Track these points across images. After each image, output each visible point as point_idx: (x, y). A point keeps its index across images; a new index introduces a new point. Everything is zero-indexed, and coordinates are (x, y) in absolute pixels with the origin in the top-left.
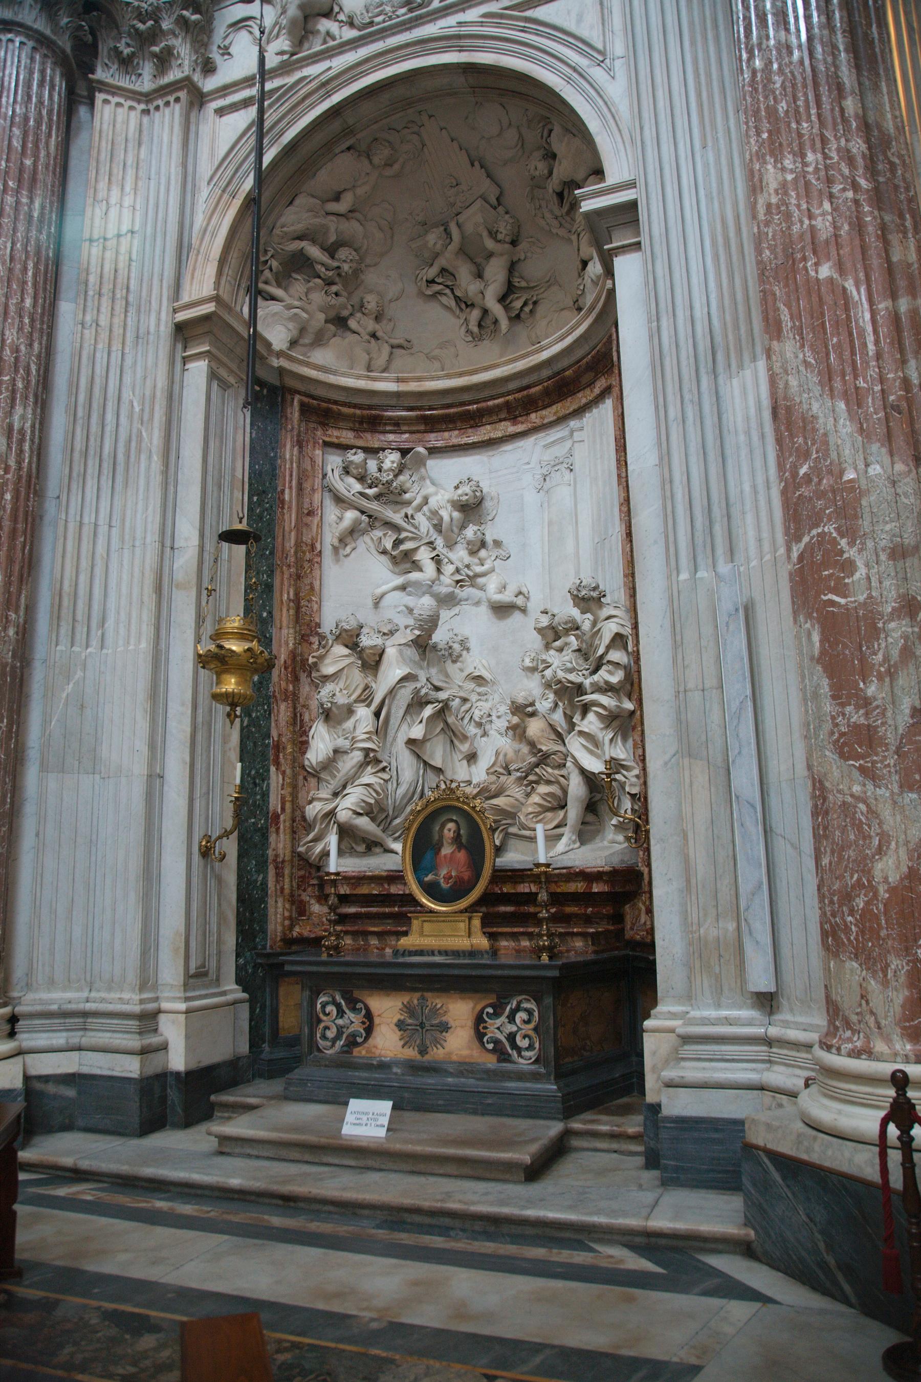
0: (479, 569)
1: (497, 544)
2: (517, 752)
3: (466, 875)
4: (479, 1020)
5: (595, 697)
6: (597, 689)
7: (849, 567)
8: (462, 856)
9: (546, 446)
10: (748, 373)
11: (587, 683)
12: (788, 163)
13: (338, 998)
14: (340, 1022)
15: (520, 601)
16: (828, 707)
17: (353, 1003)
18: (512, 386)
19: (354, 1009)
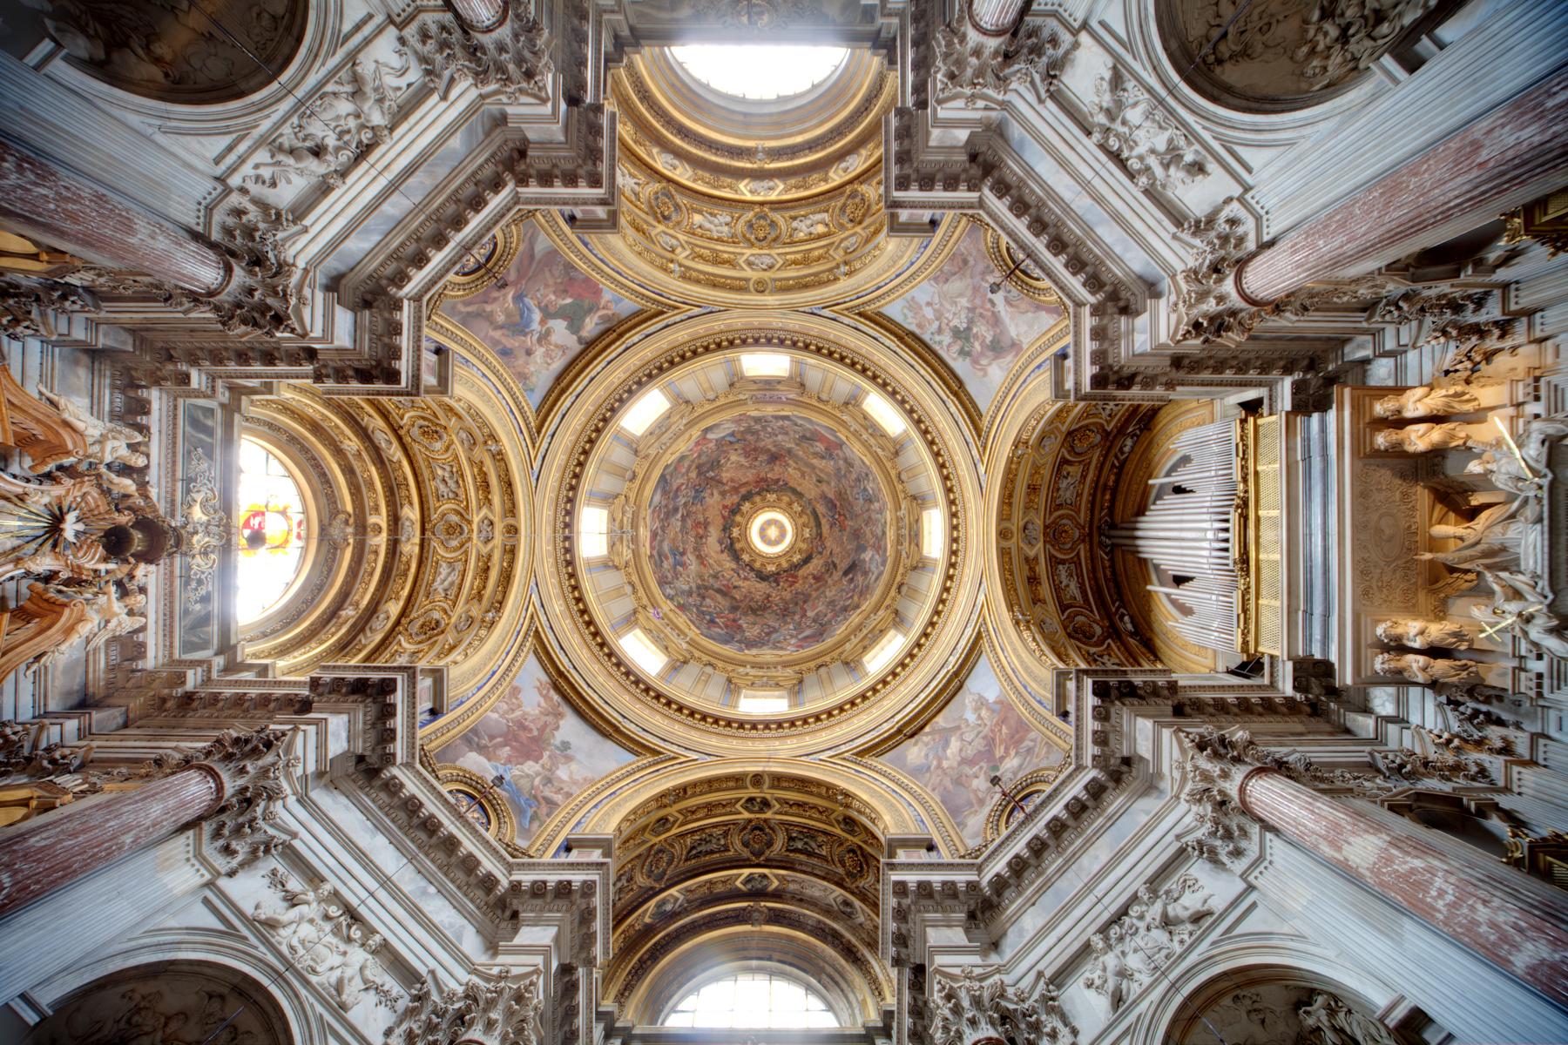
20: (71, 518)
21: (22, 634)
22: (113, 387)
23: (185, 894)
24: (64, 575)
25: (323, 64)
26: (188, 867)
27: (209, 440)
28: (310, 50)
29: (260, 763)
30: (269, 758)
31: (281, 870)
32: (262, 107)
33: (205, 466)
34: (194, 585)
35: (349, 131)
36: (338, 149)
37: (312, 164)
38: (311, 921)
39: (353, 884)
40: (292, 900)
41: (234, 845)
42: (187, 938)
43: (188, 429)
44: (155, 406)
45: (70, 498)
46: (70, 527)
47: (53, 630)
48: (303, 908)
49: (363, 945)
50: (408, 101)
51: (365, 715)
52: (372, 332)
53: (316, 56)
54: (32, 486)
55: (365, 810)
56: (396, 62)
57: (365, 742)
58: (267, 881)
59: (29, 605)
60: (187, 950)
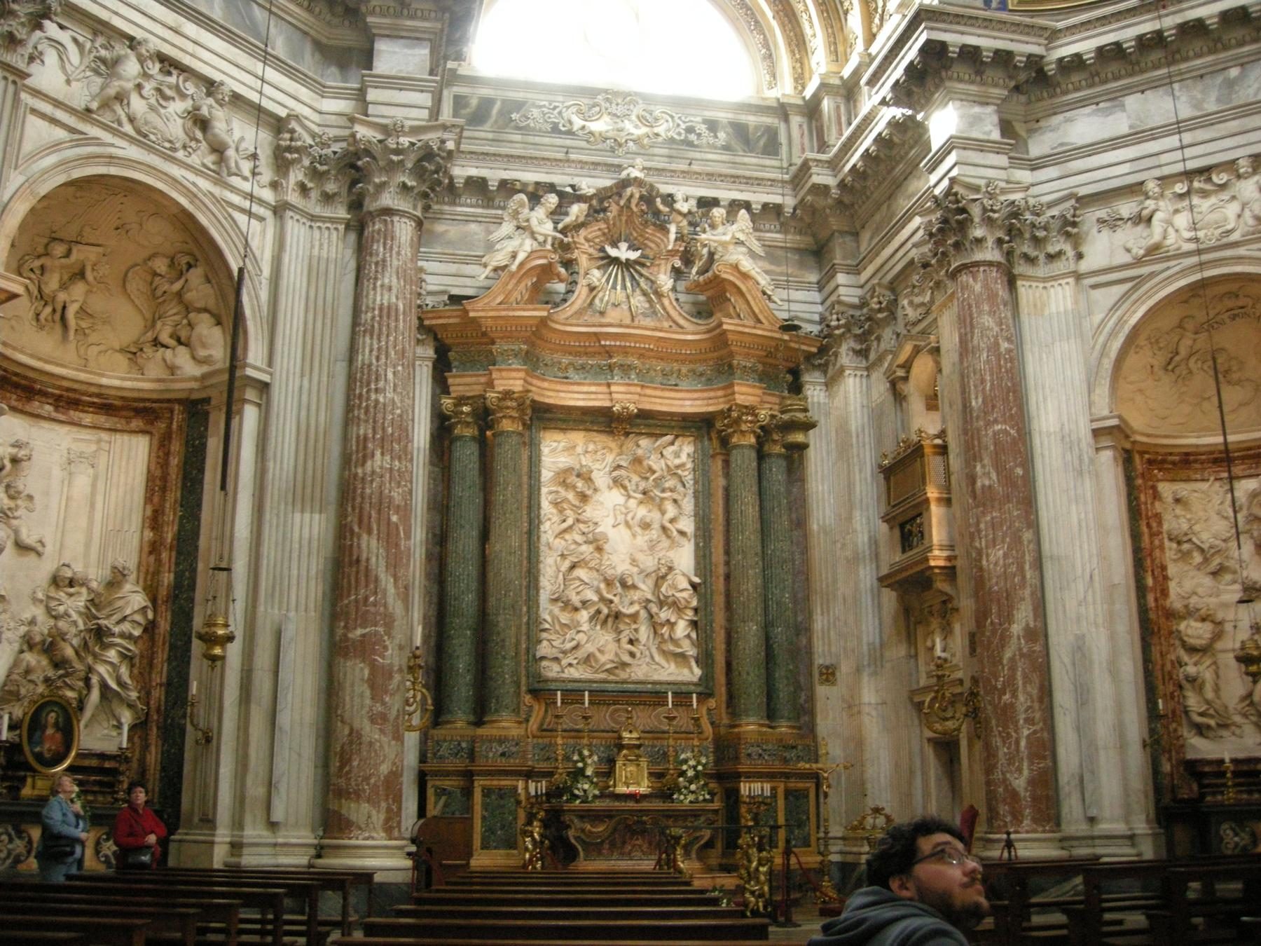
0: (16, 514)
1: (30, 497)
2: (39, 662)
3: (62, 749)
4: (98, 843)
5: (118, 640)
6: (122, 635)
7: (385, 648)
8: (59, 736)
9: (76, 440)
10: (307, 516)
11: (116, 630)
12: (388, 458)
13: (10, 829)
14: (10, 846)
15: (40, 549)
16: (368, 702)
17: (20, 833)
18: (65, 384)
19: (20, 837)
20: (613, 252)
21: (741, 306)
22: (454, 203)
23: (1076, 302)
24: (678, 264)
25: (112, 145)
26: (1052, 291)
27: (498, 106)
28: (109, 164)
29: (977, 220)
30: (976, 211)
31: (1102, 213)
32: (192, 196)
33: (535, 112)
34: (692, 137)
35: (159, 90)
36: (183, 96)
37: (219, 127)
38: (1177, 211)
39: (1164, 158)
40: (1144, 220)
41: (1051, 249)
42: (1119, 313)
43: (487, 127)
44: (473, 172)
45: (591, 251)
46: (623, 252)
47: (744, 288)
48: (1158, 216)
49: (1239, 177)
50: (81, 22)
51: (960, 80)
52: (398, 15)
53: (111, 157)
54: (582, 282)
55: (1083, 103)
56: (51, 57)
57: (996, 85)
58: (1106, 232)
59: (709, 293)
60: (1130, 317)
